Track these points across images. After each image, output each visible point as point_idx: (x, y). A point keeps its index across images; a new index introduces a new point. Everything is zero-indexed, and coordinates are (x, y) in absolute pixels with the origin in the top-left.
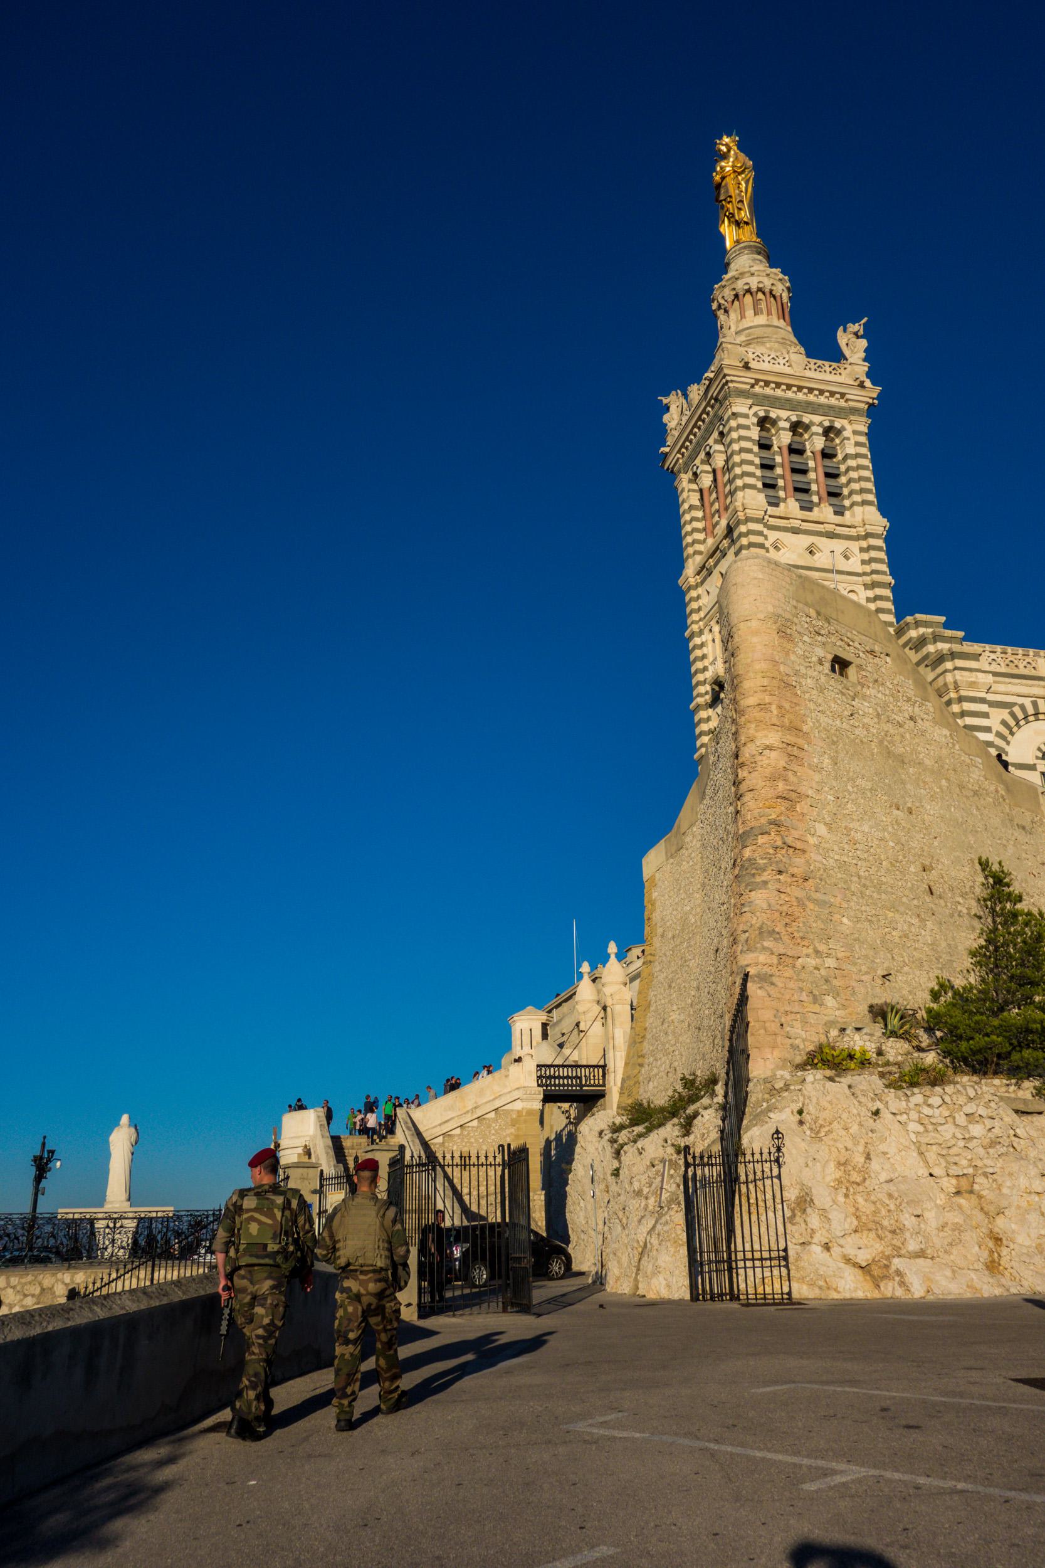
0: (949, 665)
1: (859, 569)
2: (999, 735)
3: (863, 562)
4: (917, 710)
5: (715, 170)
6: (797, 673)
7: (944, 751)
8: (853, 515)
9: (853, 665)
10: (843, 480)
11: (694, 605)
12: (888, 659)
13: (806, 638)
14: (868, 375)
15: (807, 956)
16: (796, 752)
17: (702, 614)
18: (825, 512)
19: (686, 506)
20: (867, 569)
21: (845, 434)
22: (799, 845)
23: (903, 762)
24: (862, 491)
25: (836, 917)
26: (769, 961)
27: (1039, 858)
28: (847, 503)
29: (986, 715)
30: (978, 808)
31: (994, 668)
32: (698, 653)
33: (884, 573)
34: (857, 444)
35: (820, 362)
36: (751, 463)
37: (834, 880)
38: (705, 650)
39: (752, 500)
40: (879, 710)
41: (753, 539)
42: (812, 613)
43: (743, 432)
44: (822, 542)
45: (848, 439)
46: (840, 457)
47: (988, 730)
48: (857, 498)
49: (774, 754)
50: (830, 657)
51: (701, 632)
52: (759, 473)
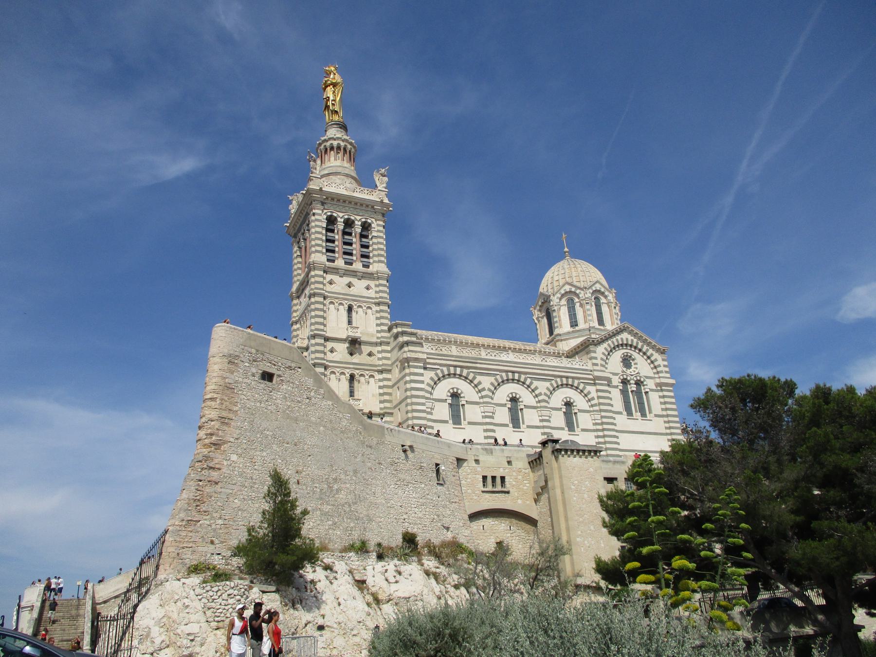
0: (406, 349)
1: (373, 295)
2: (428, 384)
3: (376, 292)
4: (312, 394)
5: (322, 82)
6: (236, 382)
7: (326, 412)
8: (373, 268)
9: (275, 376)
10: (371, 248)
11: (295, 308)
12: (299, 370)
13: (247, 364)
14: (387, 196)
15: (206, 519)
16: (226, 421)
17: (298, 313)
18: (358, 266)
19: (295, 255)
20: (378, 295)
21: (373, 225)
22: (217, 466)
23: (296, 420)
24: (379, 255)
25: (231, 499)
26: (181, 524)
27: (377, 461)
28: (371, 261)
29: (422, 375)
30: (341, 439)
31: (429, 351)
32: (295, 333)
33: (386, 298)
34: (378, 231)
35: (362, 188)
36: (321, 239)
37: (234, 482)
38: (298, 332)
39: (319, 258)
40: (287, 395)
41: (317, 279)
42: (254, 351)
43: (318, 223)
44: (354, 281)
45: (374, 228)
46: (370, 237)
47: (422, 382)
48: (376, 259)
49: (213, 423)
50: (261, 372)
51: (296, 323)
52: (324, 244)
